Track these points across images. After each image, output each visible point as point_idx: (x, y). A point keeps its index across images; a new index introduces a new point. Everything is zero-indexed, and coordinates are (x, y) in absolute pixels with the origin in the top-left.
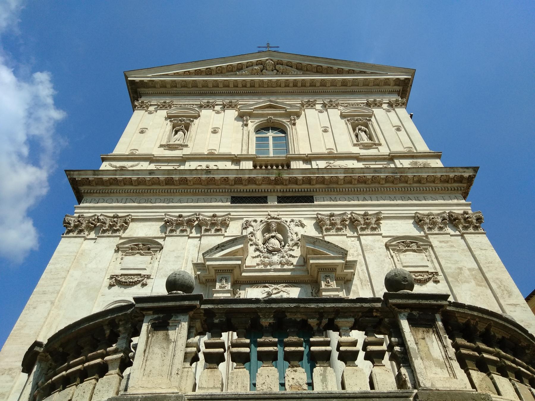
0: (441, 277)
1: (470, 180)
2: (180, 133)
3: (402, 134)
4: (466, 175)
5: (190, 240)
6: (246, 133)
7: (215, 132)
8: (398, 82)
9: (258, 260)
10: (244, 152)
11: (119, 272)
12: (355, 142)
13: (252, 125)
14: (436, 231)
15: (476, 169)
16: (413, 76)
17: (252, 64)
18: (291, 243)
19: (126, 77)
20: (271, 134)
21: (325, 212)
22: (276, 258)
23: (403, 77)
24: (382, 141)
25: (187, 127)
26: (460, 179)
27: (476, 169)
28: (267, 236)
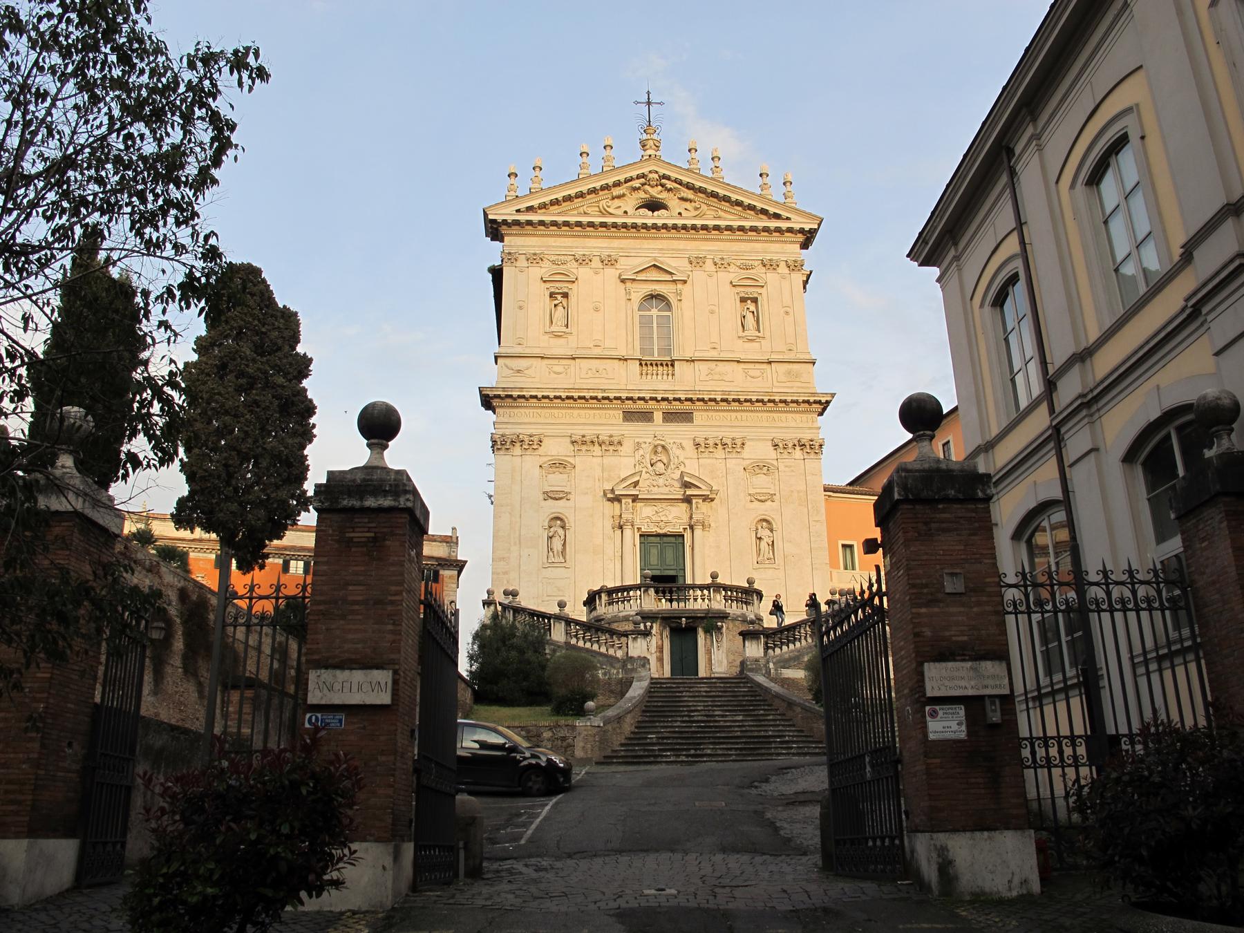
0: (776, 498)
1: (828, 403)
2: (560, 308)
3: (790, 319)
4: (823, 400)
5: (595, 459)
6: (629, 312)
7: (597, 310)
8: (802, 231)
9: (648, 482)
10: (631, 352)
11: (548, 489)
12: (741, 334)
13: (637, 297)
14: (785, 455)
15: (833, 395)
16: (819, 225)
17: (631, 179)
18: (672, 466)
19: (486, 215)
20: (654, 312)
21: (700, 435)
22: (661, 481)
23: (807, 227)
24: (767, 334)
25: (565, 295)
26: (819, 402)
27: (833, 395)
28: (655, 459)
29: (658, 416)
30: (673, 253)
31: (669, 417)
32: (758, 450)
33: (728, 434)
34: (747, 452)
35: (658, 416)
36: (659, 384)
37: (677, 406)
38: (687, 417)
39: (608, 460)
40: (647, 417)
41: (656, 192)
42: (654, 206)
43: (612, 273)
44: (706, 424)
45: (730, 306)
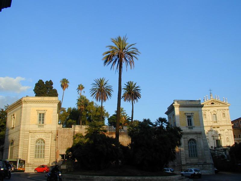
29: (216, 127)
30: (215, 109)
31: (217, 128)
32: (226, 130)
33: (223, 129)
34: (225, 131)
35: (216, 127)
36: (216, 124)
37: (218, 126)
38: (219, 127)
39: (212, 132)
40: (215, 128)
41: (213, 102)
42: (213, 103)
43: (209, 112)
44: (221, 128)
45: (222, 115)
